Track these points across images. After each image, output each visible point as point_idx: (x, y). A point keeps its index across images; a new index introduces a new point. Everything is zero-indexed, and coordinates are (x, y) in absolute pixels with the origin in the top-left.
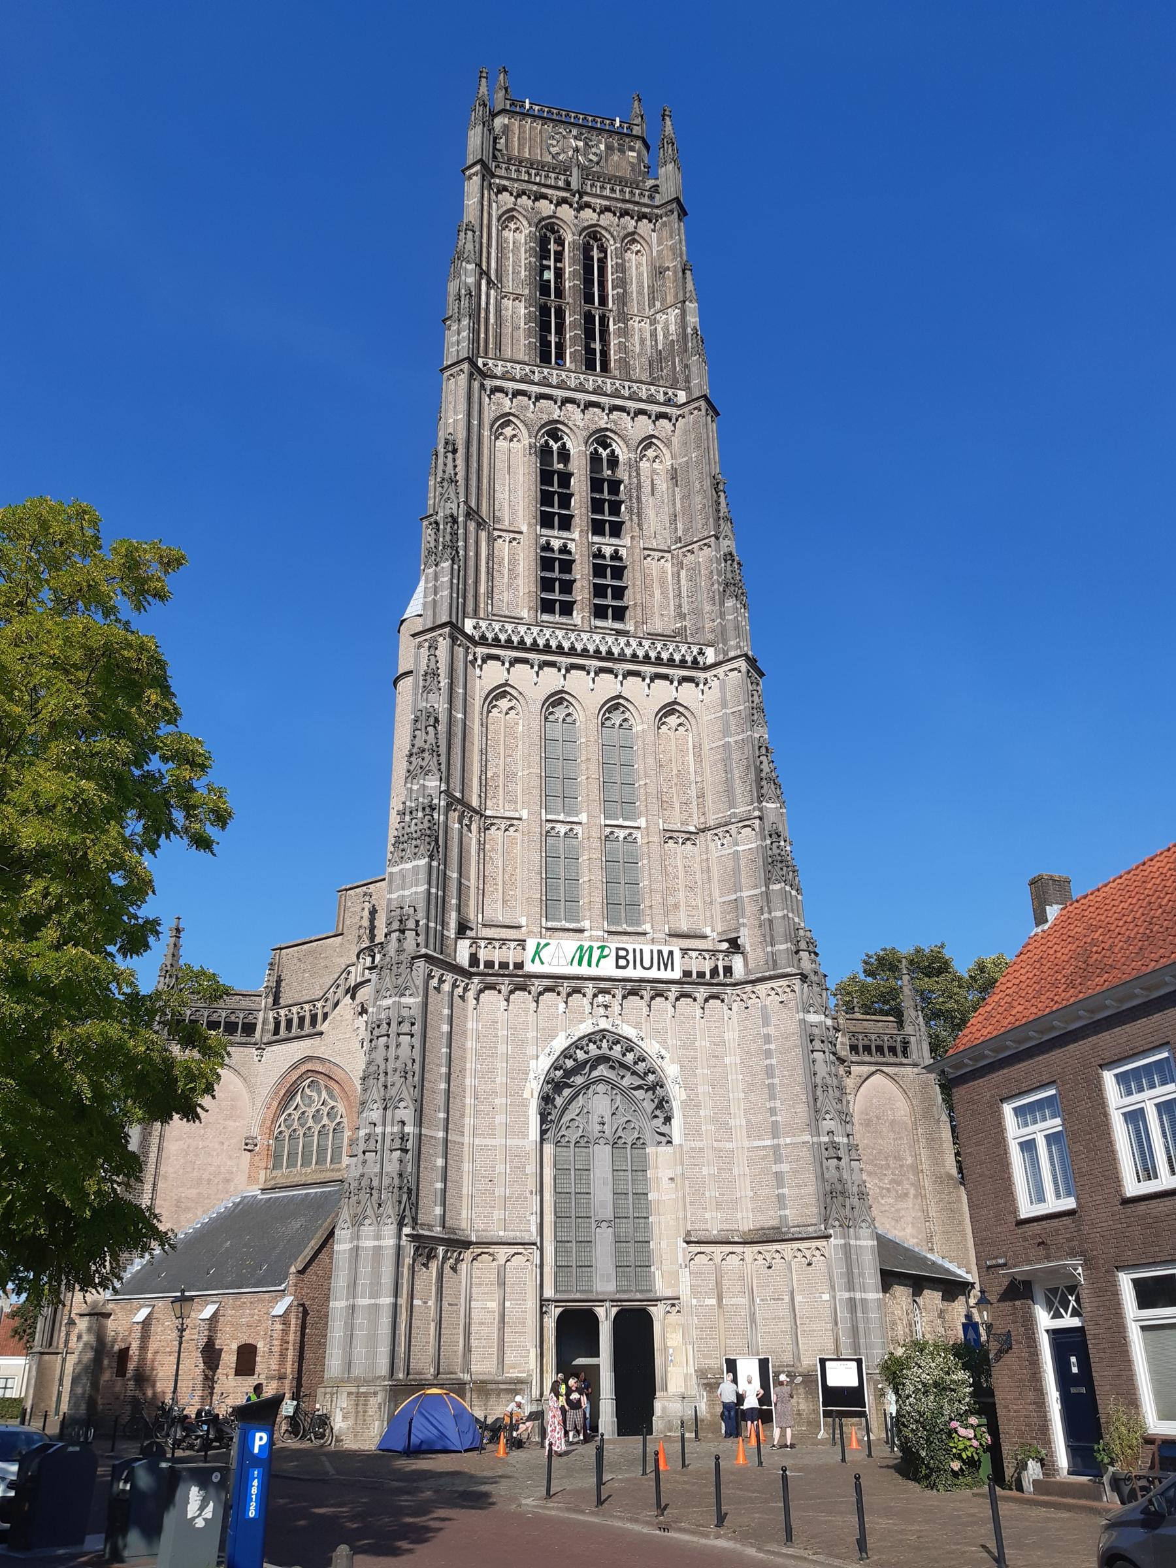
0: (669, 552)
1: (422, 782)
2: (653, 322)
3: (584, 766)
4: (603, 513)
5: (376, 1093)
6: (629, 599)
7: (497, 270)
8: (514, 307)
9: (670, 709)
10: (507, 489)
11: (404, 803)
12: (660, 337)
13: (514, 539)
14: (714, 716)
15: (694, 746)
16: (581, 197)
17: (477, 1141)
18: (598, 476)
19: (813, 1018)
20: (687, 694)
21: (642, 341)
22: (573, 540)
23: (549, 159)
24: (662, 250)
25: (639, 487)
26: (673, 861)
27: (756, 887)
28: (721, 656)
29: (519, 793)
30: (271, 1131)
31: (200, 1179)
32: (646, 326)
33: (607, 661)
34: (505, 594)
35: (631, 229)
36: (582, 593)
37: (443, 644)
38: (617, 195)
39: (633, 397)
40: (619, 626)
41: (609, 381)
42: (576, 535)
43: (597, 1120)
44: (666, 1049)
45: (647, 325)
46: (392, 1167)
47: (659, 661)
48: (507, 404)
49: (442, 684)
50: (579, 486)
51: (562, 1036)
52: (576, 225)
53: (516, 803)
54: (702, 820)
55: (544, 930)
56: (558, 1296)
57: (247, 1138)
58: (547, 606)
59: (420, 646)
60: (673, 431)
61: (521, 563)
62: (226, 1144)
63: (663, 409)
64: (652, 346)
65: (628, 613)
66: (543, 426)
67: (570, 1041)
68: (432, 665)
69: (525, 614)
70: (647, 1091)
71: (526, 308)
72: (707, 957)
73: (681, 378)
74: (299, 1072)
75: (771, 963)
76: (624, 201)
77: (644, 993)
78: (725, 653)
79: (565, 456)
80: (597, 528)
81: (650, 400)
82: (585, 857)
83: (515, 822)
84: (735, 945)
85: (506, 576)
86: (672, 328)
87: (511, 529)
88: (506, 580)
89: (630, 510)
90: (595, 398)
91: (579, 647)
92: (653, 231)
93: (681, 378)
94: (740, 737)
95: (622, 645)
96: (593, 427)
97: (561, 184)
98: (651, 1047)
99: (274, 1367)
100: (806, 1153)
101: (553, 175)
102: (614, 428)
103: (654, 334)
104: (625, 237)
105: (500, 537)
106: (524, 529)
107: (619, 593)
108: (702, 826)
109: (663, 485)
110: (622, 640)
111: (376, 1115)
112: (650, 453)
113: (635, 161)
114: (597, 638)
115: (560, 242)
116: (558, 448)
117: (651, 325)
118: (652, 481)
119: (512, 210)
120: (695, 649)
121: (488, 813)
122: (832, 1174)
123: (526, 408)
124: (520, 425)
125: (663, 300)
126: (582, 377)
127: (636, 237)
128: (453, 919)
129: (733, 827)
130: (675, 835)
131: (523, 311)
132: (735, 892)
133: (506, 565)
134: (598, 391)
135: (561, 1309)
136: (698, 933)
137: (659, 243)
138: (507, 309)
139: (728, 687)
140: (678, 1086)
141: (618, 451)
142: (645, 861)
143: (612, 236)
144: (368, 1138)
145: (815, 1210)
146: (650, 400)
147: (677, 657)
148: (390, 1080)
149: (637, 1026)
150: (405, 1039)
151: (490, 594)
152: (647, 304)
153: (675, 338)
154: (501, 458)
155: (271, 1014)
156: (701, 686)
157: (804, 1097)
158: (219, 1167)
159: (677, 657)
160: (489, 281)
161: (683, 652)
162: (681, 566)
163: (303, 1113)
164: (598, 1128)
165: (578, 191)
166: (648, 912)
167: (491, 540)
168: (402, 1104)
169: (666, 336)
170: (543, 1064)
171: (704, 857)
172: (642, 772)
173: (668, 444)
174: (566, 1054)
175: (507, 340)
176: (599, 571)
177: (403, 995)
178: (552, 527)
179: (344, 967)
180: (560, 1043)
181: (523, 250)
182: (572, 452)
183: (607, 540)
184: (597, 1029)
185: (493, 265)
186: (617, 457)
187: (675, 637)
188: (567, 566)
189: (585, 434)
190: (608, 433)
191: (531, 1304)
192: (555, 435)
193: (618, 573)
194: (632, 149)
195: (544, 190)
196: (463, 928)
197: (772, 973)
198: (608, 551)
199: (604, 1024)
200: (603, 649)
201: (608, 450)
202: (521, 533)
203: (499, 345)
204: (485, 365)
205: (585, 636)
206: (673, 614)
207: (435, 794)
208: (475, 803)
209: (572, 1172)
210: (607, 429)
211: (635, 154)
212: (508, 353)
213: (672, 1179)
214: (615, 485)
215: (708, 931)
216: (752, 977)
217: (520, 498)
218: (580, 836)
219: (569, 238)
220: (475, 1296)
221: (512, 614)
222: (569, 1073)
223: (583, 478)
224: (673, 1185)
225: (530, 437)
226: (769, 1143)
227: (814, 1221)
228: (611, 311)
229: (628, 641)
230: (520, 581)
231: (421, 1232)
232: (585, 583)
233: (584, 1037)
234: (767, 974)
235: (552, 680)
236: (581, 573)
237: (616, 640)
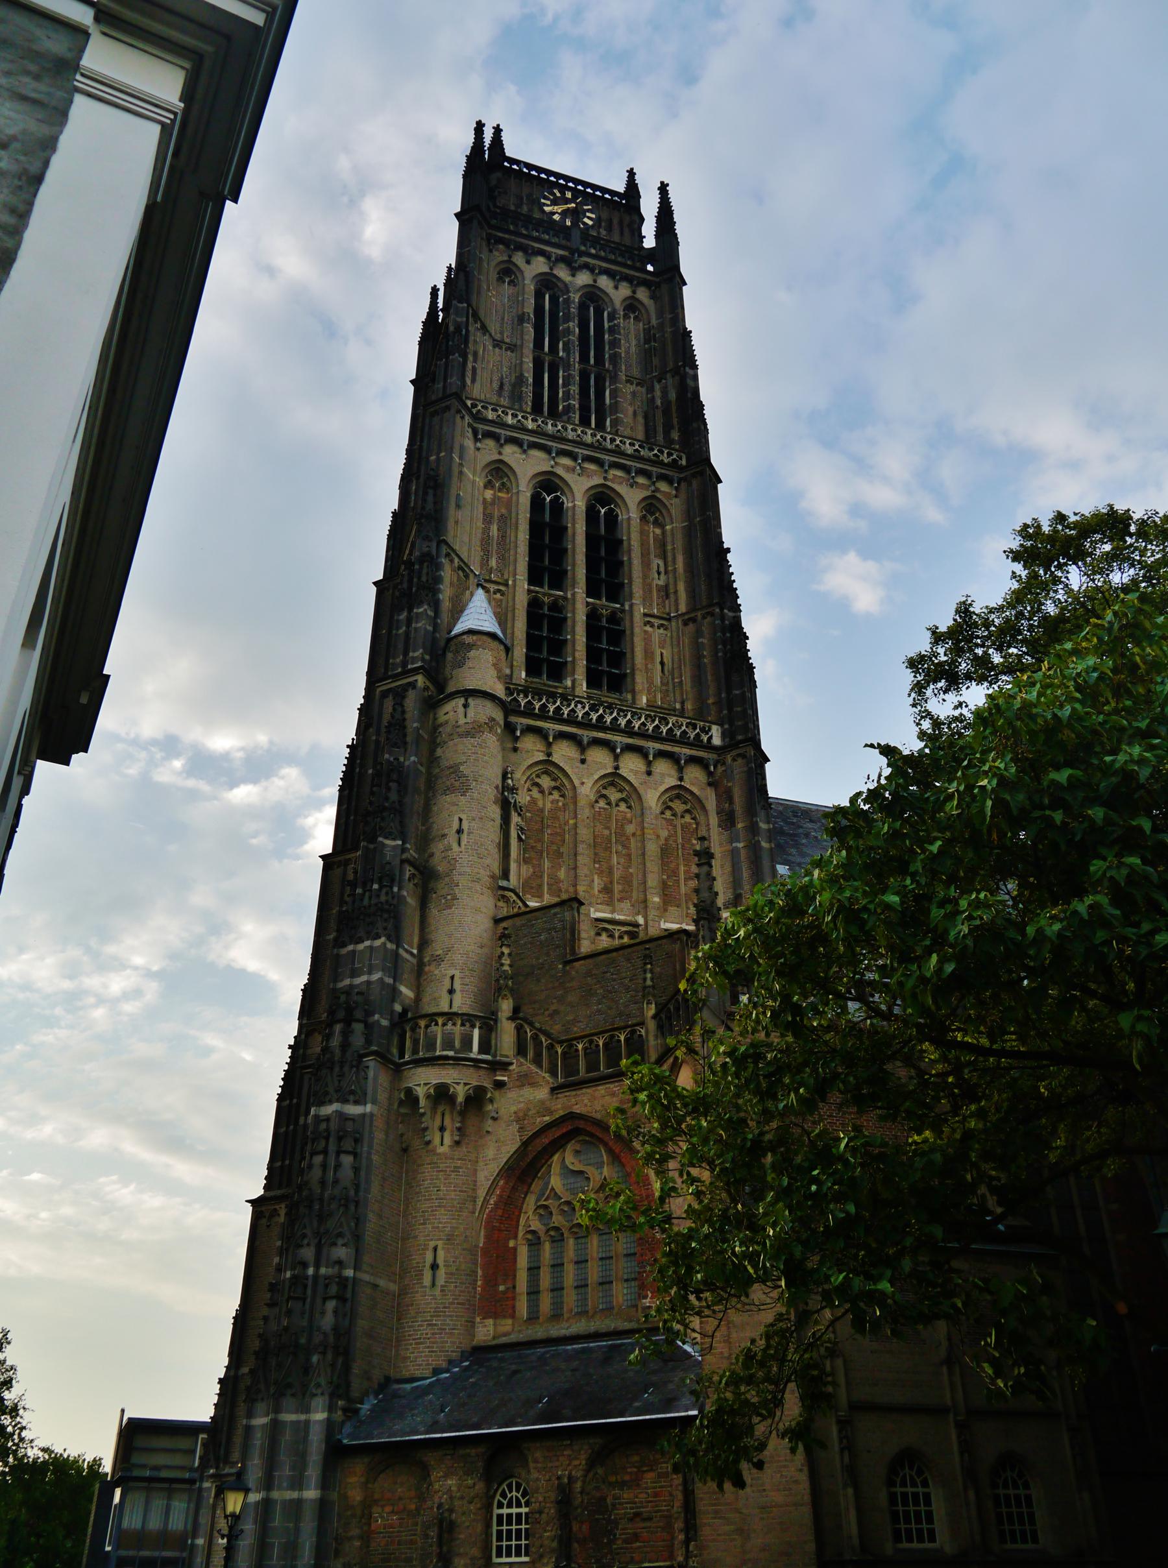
46: (327, 1321)
150: (347, 1160)
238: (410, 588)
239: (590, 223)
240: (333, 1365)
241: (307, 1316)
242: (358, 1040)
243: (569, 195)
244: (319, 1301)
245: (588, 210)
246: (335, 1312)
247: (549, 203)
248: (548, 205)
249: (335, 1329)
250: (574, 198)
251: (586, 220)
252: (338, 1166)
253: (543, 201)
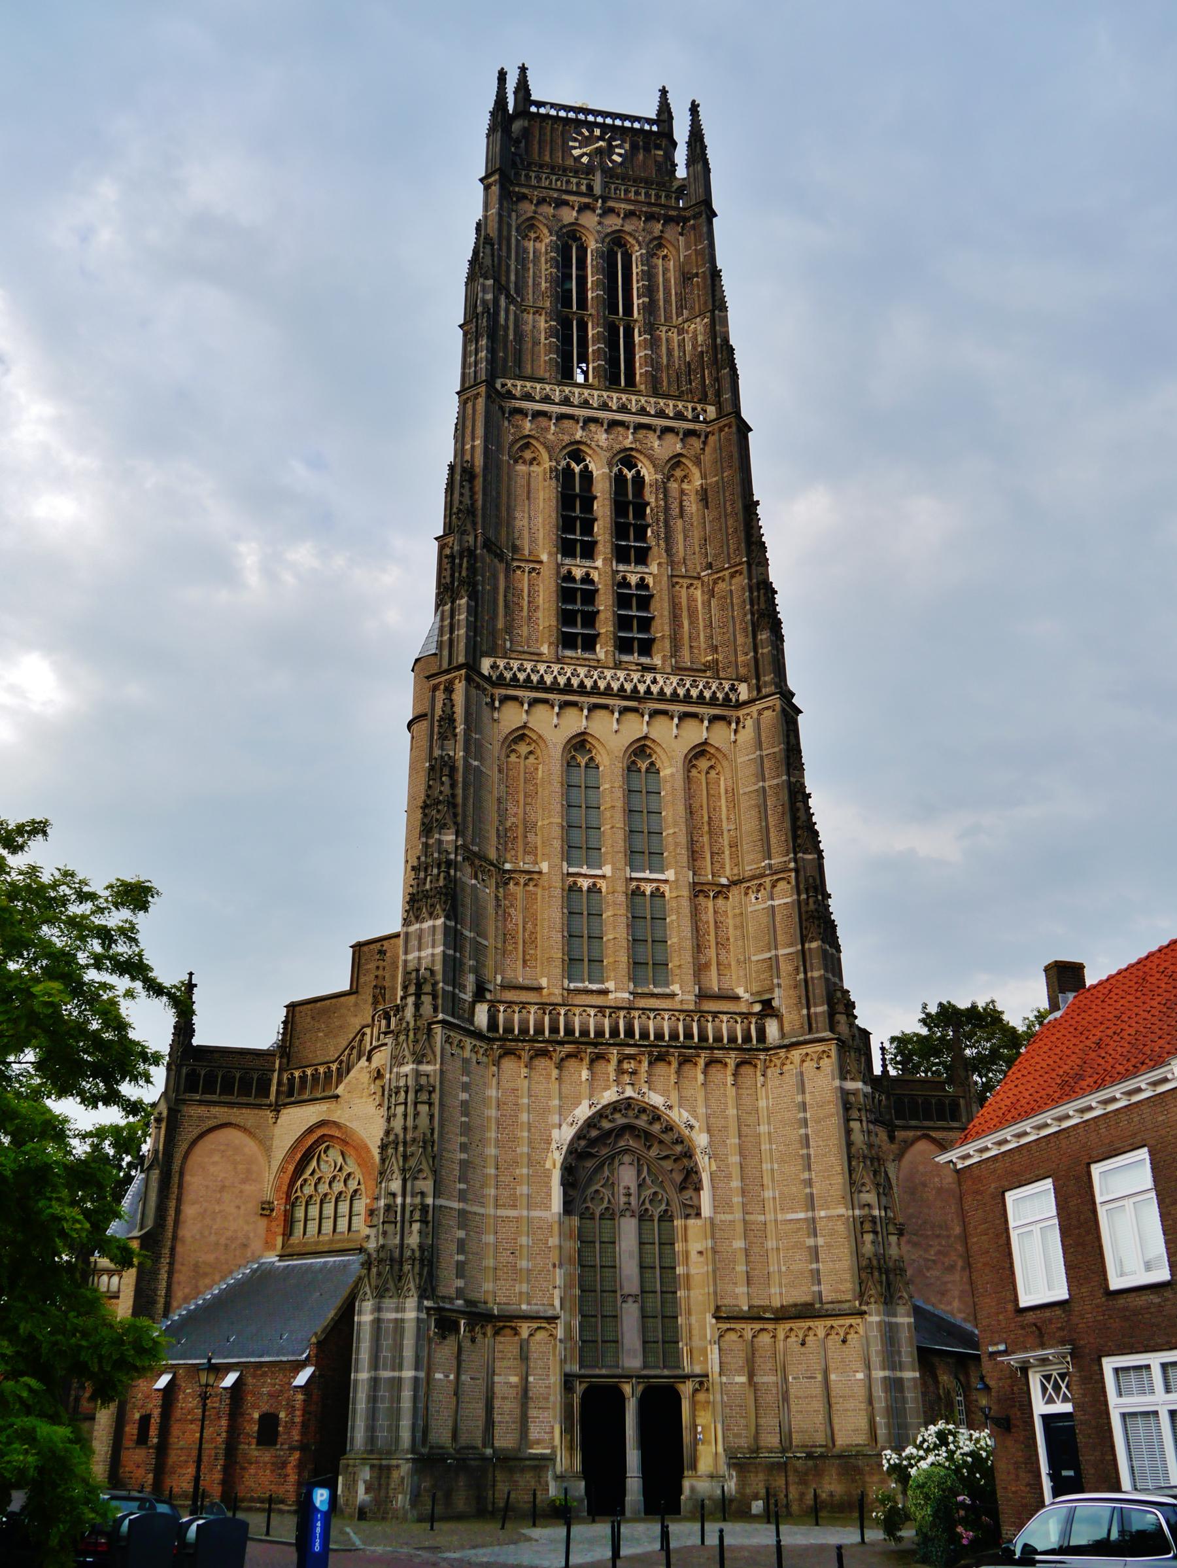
0: (699, 579)
1: (437, 836)
2: (681, 332)
3: (608, 814)
4: (628, 539)
5: (395, 1165)
7: (516, 284)
8: (534, 321)
9: (700, 751)
10: (526, 515)
11: (419, 858)
12: (689, 347)
13: (534, 569)
14: (747, 758)
15: (726, 791)
16: (604, 202)
17: (500, 1212)
18: (621, 499)
19: (851, 1085)
20: (720, 736)
21: (670, 352)
22: (596, 568)
23: (570, 162)
24: (690, 256)
25: (667, 509)
26: (704, 918)
27: (791, 945)
28: (755, 693)
29: (539, 844)
30: (288, 1196)
31: (217, 1244)
32: (675, 338)
34: (525, 628)
35: (657, 233)
36: (605, 626)
37: (460, 687)
38: (642, 198)
39: (661, 414)
40: (644, 660)
41: (634, 398)
42: (599, 563)
43: (622, 1191)
44: (696, 1118)
45: (675, 335)
46: (413, 1240)
47: (688, 698)
49: (458, 730)
50: (602, 509)
51: (585, 1103)
52: (598, 232)
53: (536, 855)
54: (735, 871)
55: (565, 993)
56: (583, 1372)
57: (263, 1203)
58: (568, 641)
59: (435, 688)
60: (703, 449)
61: (541, 594)
62: (243, 1208)
63: (691, 426)
64: (680, 357)
65: (655, 648)
66: (564, 447)
67: (594, 1110)
68: (448, 711)
69: (545, 649)
70: (675, 1160)
71: (546, 322)
72: (739, 1020)
73: (710, 393)
74: (315, 1137)
75: (806, 1027)
76: (650, 204)
77: (672, 1059)
78: (759, 690)
79: (587, 476)
80: (621, 555)
81: (679, 416)
82: (609, 913)
83: (536, 876)
84: (768, 1009)
85: (526, 608)
86: (700, 339)
87: (532, 558)
88: (525, 613)
89: (657, 535)
90: (619, 417)
91: (602, 685)
92: (681, 234)
93: (710, 393)
94: (775, 782)
95: (648, 682)
96: (617, 447)
97: (583, 188)
98: (680, 1116)
99: (296, 1438)
100: (841, 1228)
101: (574, 180)
102: (639, 447)
103: (682, 344)
104: (651, 241)
105: (519, 567)
106: (544, 557)
108: (736, 878)
109: (692, 506)
110: (649, 677)
111: (396, 1186)
112: (678, 473)
113: (660, 159)
114: (621, 674)
115: (582, 250)
116: (581, 471)
117: (679, 334)
118: (681, 502)
119: (532, 218)
120: (727, 686)
121: (508, 866)
122: (868, 1248)
123: (547, 429)
124: (541, 448)
125: (692, 308)
126: (605, 394)
127: (664, 242)
128: (470, 980)
129: (767, 879)
130: (705, 888)
131: (542, 325)
132: (770, 950)
133: (526, 598)
134: (623, 409)
135: (584, 1386)
136: (730, 993)
137: (687, 248)
138: (526, 323)
139: (763, 726)
140: (707, 1158)
141: (644, 472)
142: (674, 917)
143: (637, 241)
144: (388, 1208)
145: (849, 1285)
146: (679, 416)
147: (707, 694)
148: (409, 1150)
149: (665, 1093)
151: (509, 629)
152: (674, 311)
153: (704, 349)
154: (521, 482)
155: (285, 1076)
156: (734, 726)
157: (839, 1169)
158: (235, 1231)
159: (707, 694)
160: (508, 296)
161: (714, 688)
162: (712, 594)
163: (320, 1179)
164: (623, 1199)
165: (601, 197)
166: (677, 971)
167: (509, 571)
168: (421, 1175)
169: (694, 347)
170: (565, 1134)
171: (737, 911)
172: (670, 820)
173: (698, 462)
174: (590, 1123)
175: (527, 357)
176: (623, 601)
177: (420, 1062)
178: (574, 556)
179: (359, 1028)
180: (583, 1112)
181: (543, 259)
182: (595, 474)
183: (632, 568)
184: (622, 1096)
185: (513, 278)
186: (643, 477)
187: (705, 671)
189: (608, 455)
190: (634, 453)
191: (555, 1380)
192: (577, 455)
194: (658, 147)
195: (565, 197)
196: (480, 994)
197: (807, 1037)
198: (633, 579)
199: (629, 1092)
200: (628, 687)
201: (633, 471)
202: (541, 562)
203: (519, 363)
204: (503, 385)
205: (608, 674)
206: (703, 646)
207: (451, 848)
208: (492, 855)
209: (597, 1245)
210: (632, 449)
211: (661, 153)
212: (528, 371)
213: (700, 1253)
215: (740, 991)
216: (786, 1042)
217: (540, 525)
218: (604, 890)
219: (592, 245)
220: (497, 1371)
221: (532, 650)
222: (593, 1142)
223: (607, 503)
224: (702, 1259)
225: (551, 460)
226: (802, 1215)
227: (849, 1297)
228: (636, 321)
229: (655, 678)
230: (540, 614)
231: (441, 1305)
232: (609, 614)
233: (609, 1105)
234: (801, 1038)
236: (605, 604)
237: (643, 676)
238: (452, 582)
239: (619, 159)
240: (420, 1275)
241: (398, 1237)
242: (427, 1008)
243: (597, 132)
244: (407, 1225)
245: (617, 146)
246: (420, 1232)
247: (577, 144)
248: (575, 148)
249: (421, 1246)
250: (603, 133)
251: (615, 157)
252: (416, 1115)
253: (571, 144)
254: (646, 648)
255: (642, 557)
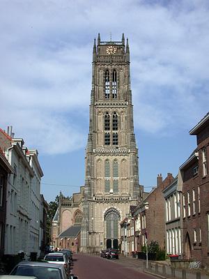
6: (119, 141)
33: (114, 154)
48: (100, 110)
58: (106, 144)
80: (114, 129)
107: (117, 140)
109: (124, 119)
170: (104, 212)
176: (114, 137)
180: (106, 209)
188: (109, 136)
192: (107, 113)
193: (117, 136)
214: (116, 121)
235: (106, 157)
236: (111, 138)
254: (117, 144)
255: (117, 129)
